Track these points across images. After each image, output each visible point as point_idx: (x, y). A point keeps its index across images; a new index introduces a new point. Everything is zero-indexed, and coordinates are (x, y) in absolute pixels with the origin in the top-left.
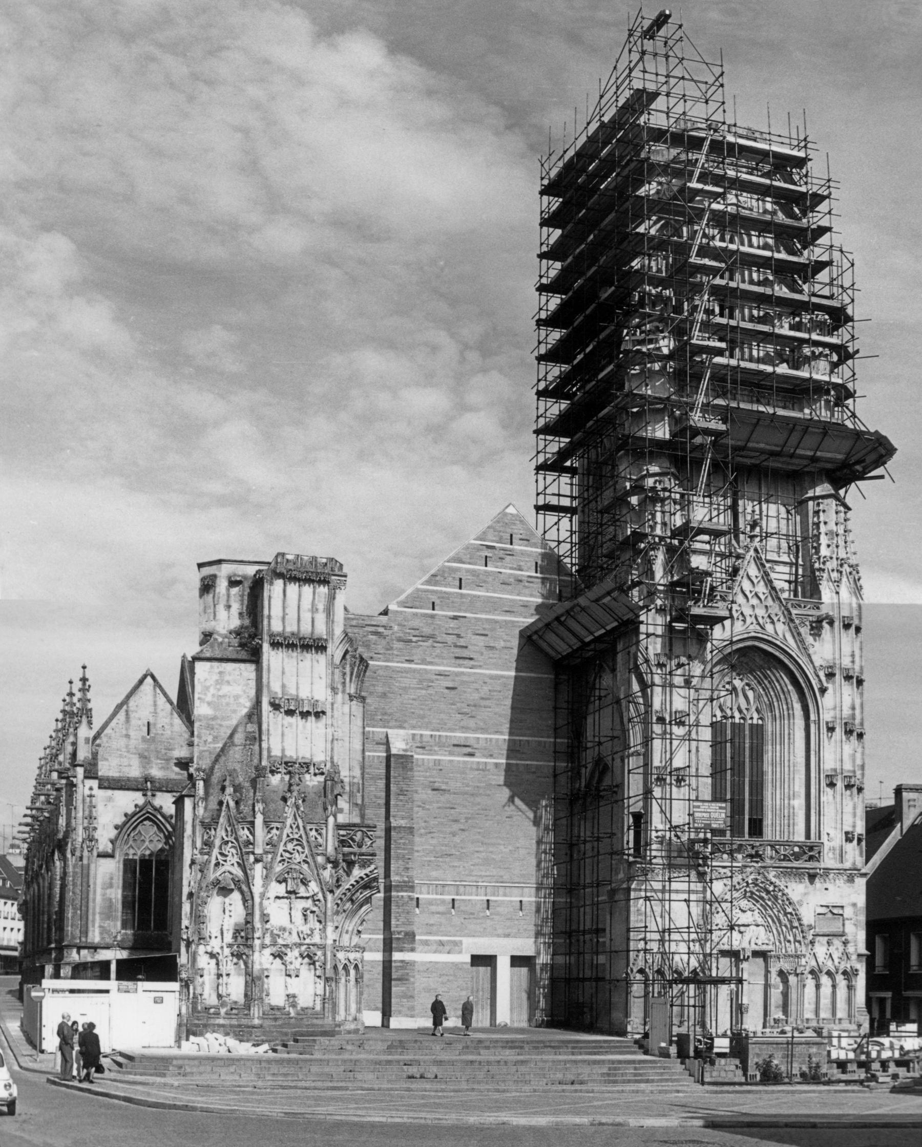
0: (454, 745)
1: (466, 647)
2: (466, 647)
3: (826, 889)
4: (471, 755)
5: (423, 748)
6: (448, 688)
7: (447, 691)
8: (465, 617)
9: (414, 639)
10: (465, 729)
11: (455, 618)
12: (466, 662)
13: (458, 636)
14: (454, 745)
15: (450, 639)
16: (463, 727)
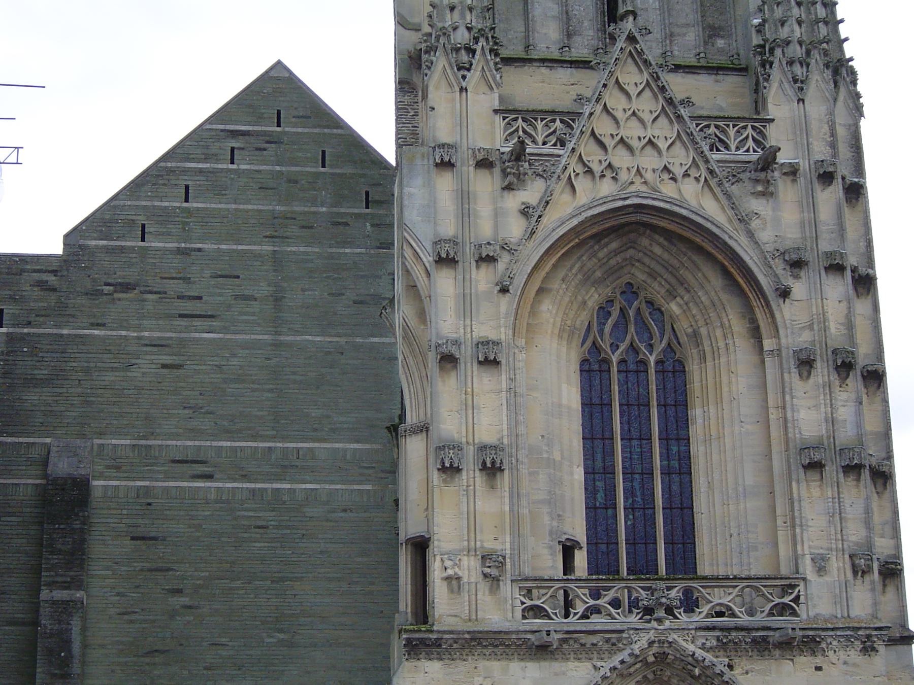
0: (174, 461)
1: (200, 298)
2: (200, 298)
3: (818, 669)
4: (209, 477)
5: (118, 468)
6: (164, 366)
7: (165, 371)
8: (199, 250)
9: (107, 289)
10: (196, 433)
11: (180, 252)
12: (197, 322)
13: (187, 280)
14: (174, 461)
15: (174, 287)
16: (192, 430)
